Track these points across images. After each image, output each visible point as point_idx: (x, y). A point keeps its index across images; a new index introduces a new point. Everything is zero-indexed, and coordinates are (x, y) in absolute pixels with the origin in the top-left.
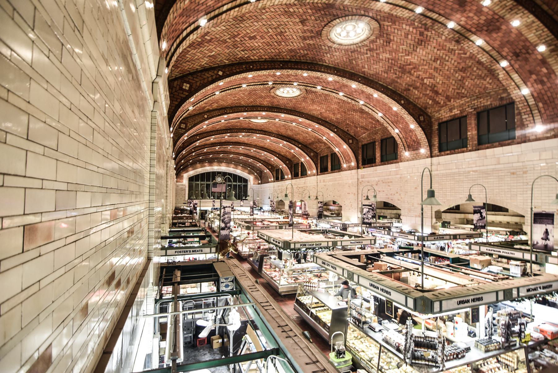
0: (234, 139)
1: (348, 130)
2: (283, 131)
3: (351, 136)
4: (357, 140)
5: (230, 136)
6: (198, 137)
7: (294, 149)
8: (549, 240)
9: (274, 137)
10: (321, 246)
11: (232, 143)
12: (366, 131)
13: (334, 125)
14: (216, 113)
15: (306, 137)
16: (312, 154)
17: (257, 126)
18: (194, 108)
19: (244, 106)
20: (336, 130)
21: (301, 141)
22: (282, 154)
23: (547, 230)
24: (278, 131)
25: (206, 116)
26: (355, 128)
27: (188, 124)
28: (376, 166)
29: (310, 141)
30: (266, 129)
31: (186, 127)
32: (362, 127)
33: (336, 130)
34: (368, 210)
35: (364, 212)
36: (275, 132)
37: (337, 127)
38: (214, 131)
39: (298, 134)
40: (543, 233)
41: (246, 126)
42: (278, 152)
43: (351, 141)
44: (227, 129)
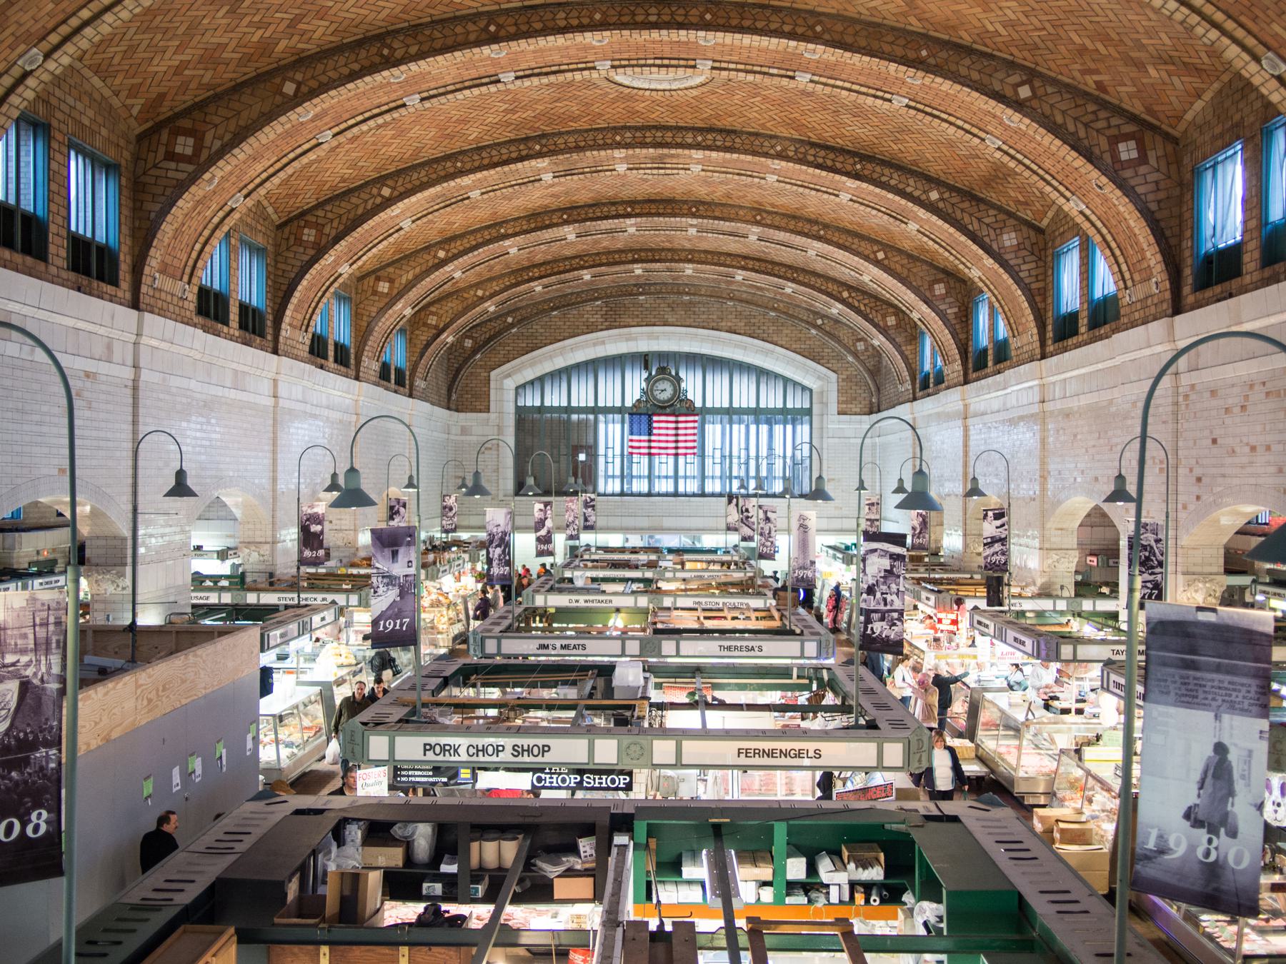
0: (581, 189)
1: (1100, 86)
2: (821, 126)
3: (1133, 118)
4: (1175, 141)
5: (569, 173)
6: (386, 192)
7: (916, 219)
8: (1233, 834)
9: (781, 156)
10: (548, 758)
11: (632, 203)
12: (1196, 82)
13: (1012, 65)
14: (342, 64)
15: (951, 144)
16: (1009, 239)
17: (673, 108)
18: (64, 58)
19: (479, 15)
20: (1025, 92)
21: (935, 169)
22: (906, 245)
23: (1220, 749)
24: (799, 127)
25: (289, 88)
26: (1134, 73)
27: (209, 137)
28: (1244, 290)
29: (980, 169)
30: (726, 123)
31: (198, 148)
32: (1163, 60)
33: (1025, 92)
34: (886, 563)
35: (871, 581)
36: (785, 133)
37: (1031, 75)
38: (462, 152)
39: (901, 131)
40: (1196, 776)
41: (614, 114)
42: (883, 238)
43: (1127, 151)
44: (527, 139)
